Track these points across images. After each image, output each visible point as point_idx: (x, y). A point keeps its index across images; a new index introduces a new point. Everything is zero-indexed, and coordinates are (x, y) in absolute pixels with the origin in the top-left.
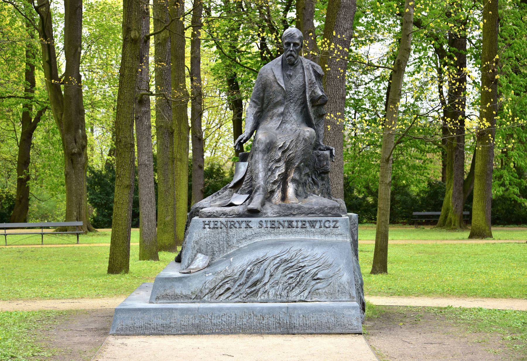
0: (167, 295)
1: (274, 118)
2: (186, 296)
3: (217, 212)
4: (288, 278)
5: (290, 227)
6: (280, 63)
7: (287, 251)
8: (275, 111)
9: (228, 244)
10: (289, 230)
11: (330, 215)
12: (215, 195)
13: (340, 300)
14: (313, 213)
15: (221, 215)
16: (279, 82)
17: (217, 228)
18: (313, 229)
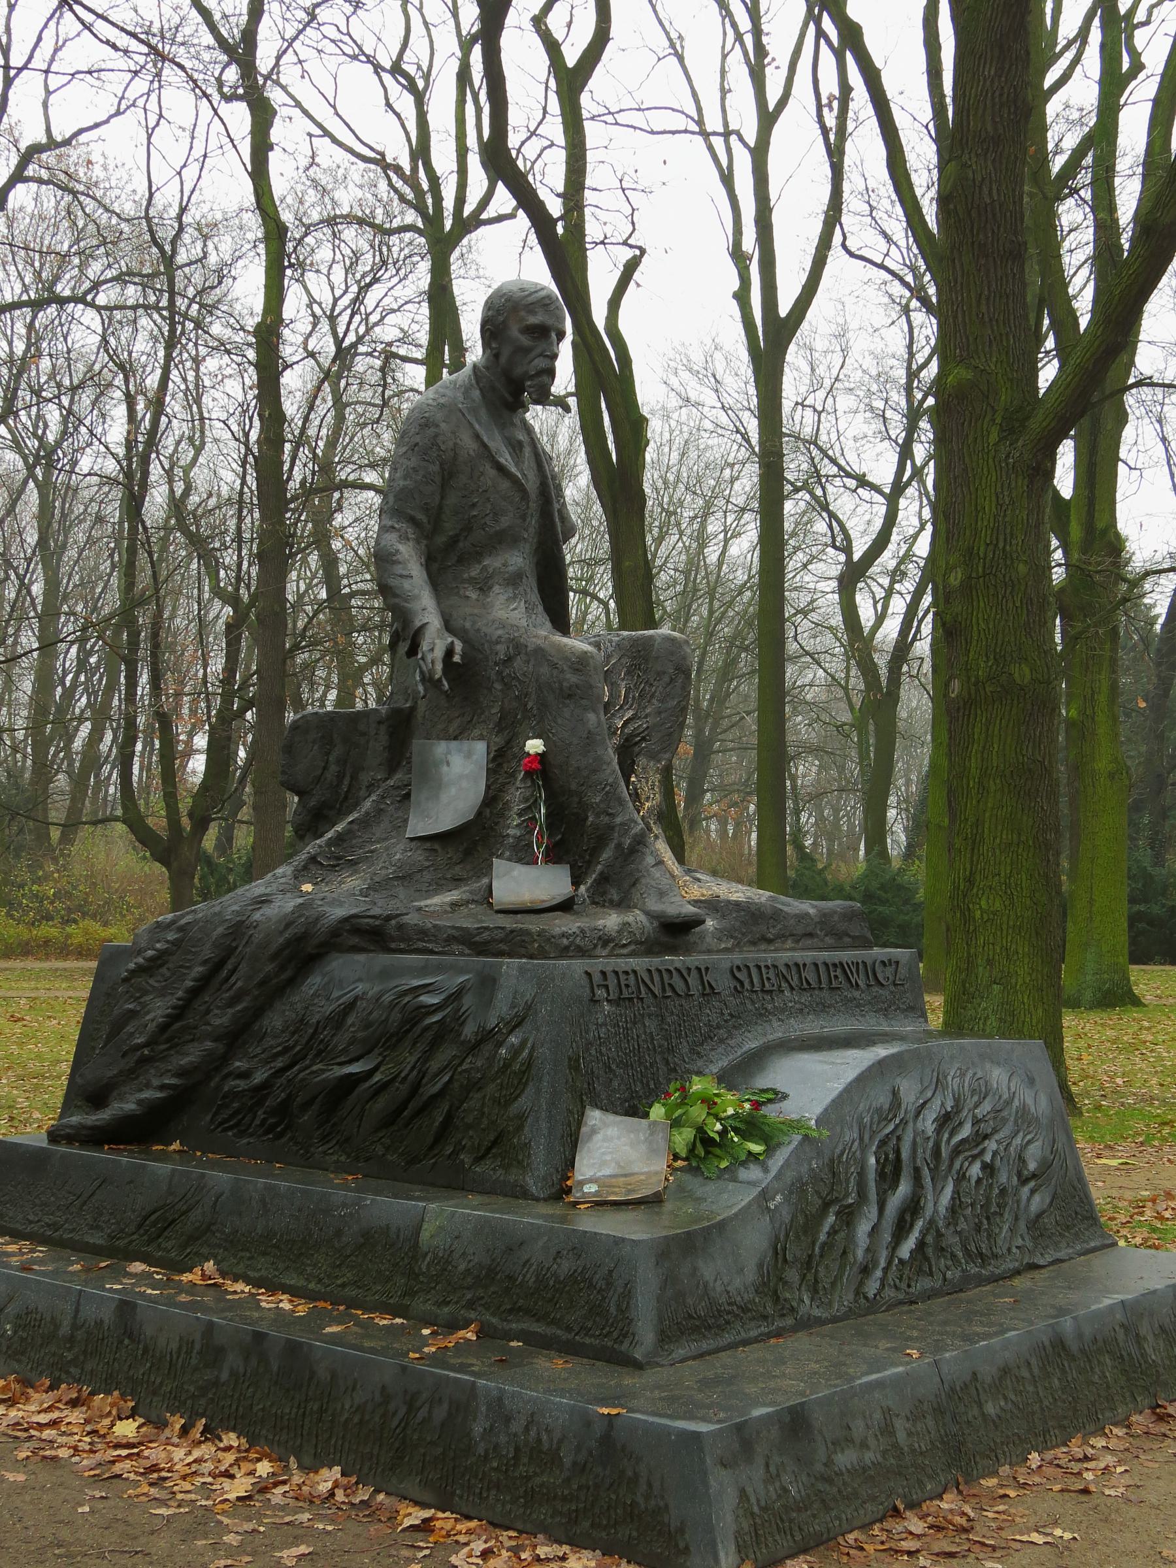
0: (690, 1316)
1: (496, 589)
2: (744, 1310)
3: (582, 931)
4: (973, 1182)
5: (805, 985)
6: (476, 394)
7: (935, 1080)
8: (493, 562)
9: (667, 1063)
10: (806, 998)
11: (847, 940)
12: (305, 868)
13: (1093, 1244)
14: (810, 935)
15: (595, 946)
16: (502, 460)
17: (630, 1000)
18: (857, 994)
